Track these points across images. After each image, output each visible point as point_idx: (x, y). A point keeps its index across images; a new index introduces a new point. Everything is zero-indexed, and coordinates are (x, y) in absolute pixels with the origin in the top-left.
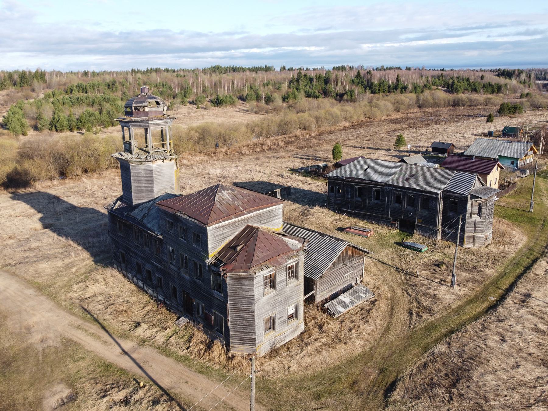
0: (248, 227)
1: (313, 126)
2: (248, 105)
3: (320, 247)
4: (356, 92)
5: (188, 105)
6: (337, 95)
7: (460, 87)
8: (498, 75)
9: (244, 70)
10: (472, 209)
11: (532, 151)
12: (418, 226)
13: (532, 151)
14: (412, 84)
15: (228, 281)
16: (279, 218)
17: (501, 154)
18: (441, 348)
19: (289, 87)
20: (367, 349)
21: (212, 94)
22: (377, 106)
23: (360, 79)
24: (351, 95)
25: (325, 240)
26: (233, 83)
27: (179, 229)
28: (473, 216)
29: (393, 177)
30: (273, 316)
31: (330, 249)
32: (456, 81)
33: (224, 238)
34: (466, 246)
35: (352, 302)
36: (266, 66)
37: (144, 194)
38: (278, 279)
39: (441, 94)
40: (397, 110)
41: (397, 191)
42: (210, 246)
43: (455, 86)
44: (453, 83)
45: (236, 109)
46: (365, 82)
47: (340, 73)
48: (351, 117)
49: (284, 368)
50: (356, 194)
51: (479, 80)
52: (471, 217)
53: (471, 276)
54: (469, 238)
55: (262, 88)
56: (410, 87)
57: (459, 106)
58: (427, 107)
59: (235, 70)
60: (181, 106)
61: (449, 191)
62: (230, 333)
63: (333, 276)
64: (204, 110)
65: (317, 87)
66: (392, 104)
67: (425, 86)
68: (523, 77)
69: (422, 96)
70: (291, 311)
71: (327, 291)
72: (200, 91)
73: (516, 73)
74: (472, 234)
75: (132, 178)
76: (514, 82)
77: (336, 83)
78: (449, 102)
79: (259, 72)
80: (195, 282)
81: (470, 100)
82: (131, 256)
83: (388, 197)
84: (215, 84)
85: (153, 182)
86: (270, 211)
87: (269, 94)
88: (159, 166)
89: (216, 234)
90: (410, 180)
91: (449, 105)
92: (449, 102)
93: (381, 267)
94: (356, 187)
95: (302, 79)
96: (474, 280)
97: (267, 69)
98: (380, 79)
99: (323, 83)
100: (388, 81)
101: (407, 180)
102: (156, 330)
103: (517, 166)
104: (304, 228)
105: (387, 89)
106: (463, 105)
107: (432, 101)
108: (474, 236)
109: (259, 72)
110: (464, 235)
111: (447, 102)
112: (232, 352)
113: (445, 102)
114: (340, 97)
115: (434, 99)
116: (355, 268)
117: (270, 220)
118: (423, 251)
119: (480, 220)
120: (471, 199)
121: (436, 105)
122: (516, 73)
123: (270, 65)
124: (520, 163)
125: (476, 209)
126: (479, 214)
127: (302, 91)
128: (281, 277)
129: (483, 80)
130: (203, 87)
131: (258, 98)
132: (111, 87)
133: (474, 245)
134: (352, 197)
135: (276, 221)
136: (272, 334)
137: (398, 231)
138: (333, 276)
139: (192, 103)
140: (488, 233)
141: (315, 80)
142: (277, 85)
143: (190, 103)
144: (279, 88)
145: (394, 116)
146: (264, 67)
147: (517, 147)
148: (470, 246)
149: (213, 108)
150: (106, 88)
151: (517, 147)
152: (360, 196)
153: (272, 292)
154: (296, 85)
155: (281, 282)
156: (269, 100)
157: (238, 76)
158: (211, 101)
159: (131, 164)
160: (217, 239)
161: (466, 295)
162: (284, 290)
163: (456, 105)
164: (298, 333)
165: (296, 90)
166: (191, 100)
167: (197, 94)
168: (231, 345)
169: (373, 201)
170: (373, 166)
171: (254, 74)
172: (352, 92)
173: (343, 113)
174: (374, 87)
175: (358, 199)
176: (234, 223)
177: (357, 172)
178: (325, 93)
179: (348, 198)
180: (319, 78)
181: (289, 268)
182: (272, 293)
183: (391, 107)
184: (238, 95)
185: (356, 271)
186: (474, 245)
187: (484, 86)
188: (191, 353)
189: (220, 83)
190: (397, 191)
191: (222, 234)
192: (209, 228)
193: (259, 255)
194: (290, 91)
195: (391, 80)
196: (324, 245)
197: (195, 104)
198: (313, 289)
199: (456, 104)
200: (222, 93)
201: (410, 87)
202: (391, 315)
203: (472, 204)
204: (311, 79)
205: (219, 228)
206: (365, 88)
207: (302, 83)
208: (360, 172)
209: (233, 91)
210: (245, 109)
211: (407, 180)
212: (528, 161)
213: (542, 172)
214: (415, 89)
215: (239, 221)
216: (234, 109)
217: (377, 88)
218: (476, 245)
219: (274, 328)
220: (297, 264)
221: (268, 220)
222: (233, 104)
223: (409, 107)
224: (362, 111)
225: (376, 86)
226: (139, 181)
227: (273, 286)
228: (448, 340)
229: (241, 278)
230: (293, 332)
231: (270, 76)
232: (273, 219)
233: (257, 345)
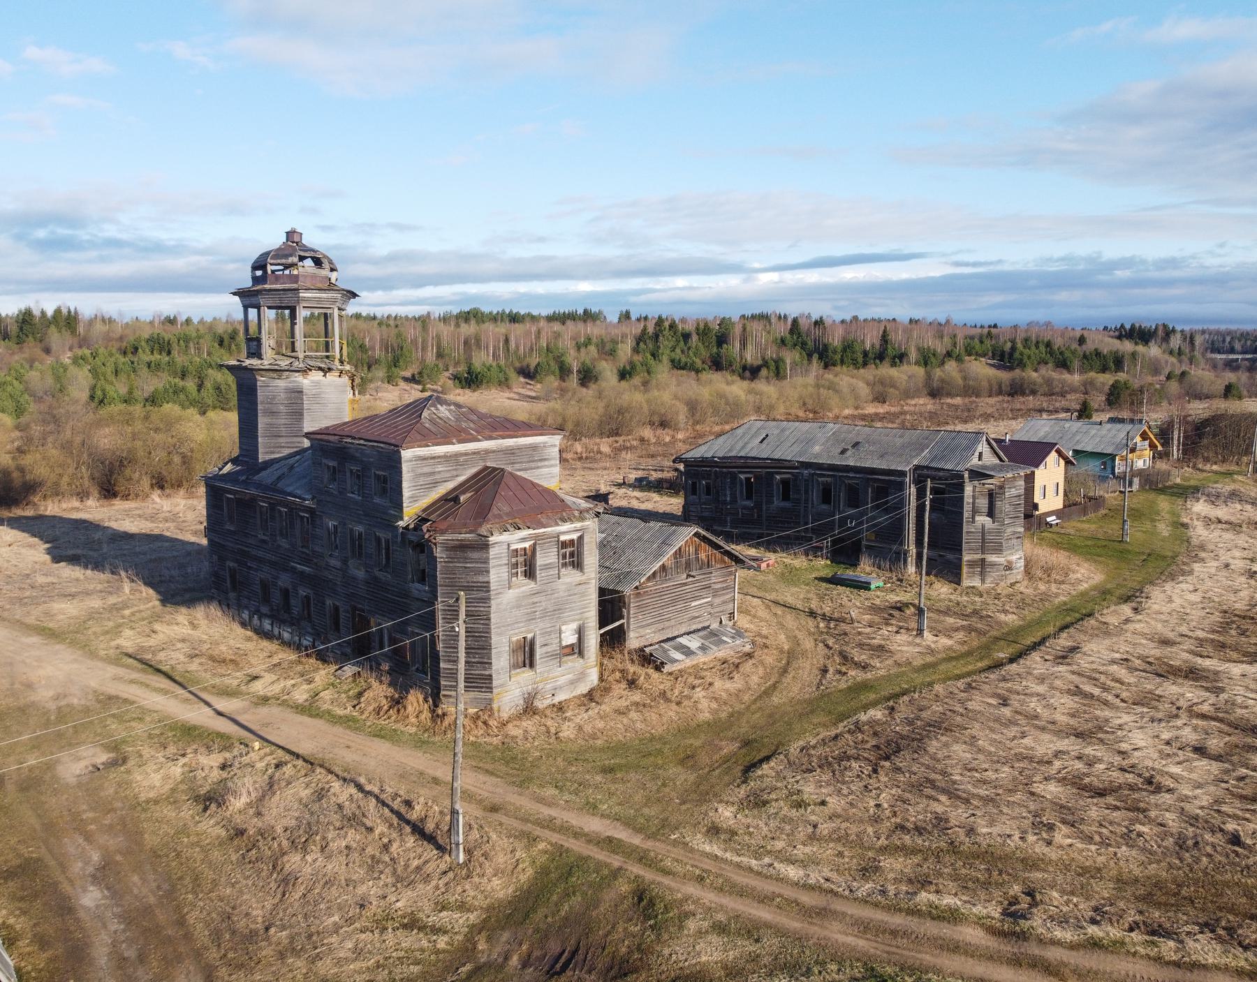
0: (486, 468)
1: (682, 418)
2: (539, 386)
3: (639, 539)
4: (788, 361)
5: (402, 384)
6: (744, 368)
7: (1029, 357)
8: (1119, 337)
9: (534, 319)
10: (974, 503)
11: (1147, 443)
12: (868, 547)
13: (1147, 443)
14: (918, 349)
15: (439, 553)
16: (552, 466)
17: (1079, 448)
18: (877, 714)
19: (636, 350)
20: (724, 715)
21: (457, 364)
22: (832, 387)
23: (799, 335)
24: (777, 368)
25: (651, 529)
26: (507, 341)
27: (348, 474)
28: (977, 518)
29: (817, 449)
30: (530, 636)
31: (660, 541)
32: (1019, 345)
33: (436, 484)
34: (966, 582)
35: (703, 648)
36: (585, 311)
37: (281, 440)
38: (540, 561)
39: (982, 369)
40: (880, 399)
41: (824, 476)
42: (406, 493)
43: (1017, 355)
44: (1013, 348)
45: (512, 395)
46: (810, 344)
47: (756, 327)
48: (771, 407)
49: (548, 732)
50: (741, 492)
51: (1075, 346)
52: (973, 518)
53: (965, 623)
54: (972, 564)
55: (573, 352)
56: (913, 355)
57: (1023, 394)
58: (949, 395)
59: (514, 318)
60: (386, 385)
61: (927, 467)
62: (442, 665)
63: (667, 598)
65: (700, 351)
66: (868, 384)
67: (949, 354)
68: (1176, 342)
69: (938, 373)
70: (570, 638)
71: (653, 628)
72: (431, 357)
73: (1160, 332)
74: (979, 556)
75: (260, 407)
76: (1154, 350)
77: (744, 344)
78: (1000, 387)
79: (569, 323)
80: (376, 578)
81: (1049, 382)
82: (250, 568)
83: (806, 492)
84: (466, 343)
85: (301, 414)
86: (534, 448)
87: (588, 362)
88: (317, 384)
89: (420, 471)
90: (849, 453)
91: (1000, 393)
92: (1000, 387)
93: (779, 611)
94: (742, 476)
95: (666, 332)
96: (970, 629)
97: (588, 316)
98: (844, 339)
99: (714, 343)
100: (863, 342)
101: (843, 452)
102: (293, 682)
103: (1113, 473)
104: (648, 625)
105: (860, 360)
106: (1034, 392)
107: (960, 382)
108: (983, 560)
109: (569, 323)
110: (960, 559)
111: (995, 387)
112: (446, 706)
113: (991, 385)
114: (751, 372)
115: (965, 378)
117: (533, 465)
118: (873, 587)
119: (993, 526)
120: (971, 478)
121: (970, 390)
122: (1160, 332)
123: (595, 309)
124: (1119, 467)
125: (983, 503)
126: (991, 514)
127: (665, 359)
128: (547, 557)
129: (1084, 347)
130: (439, 347)
131: (564, 371)
132: (226, 343)
133: (983, 581)
134: (734, 500)
136: (526, 675)
137: (829, 562)
138: (667, 598)
140: (1014, 558)
141: (695, 338)
142: (608, 347)
143: (406, 379)
144: (612, 353)
145: (871, 409)
146: (580, 311)
147: (1114, 432)
148: (976, 582)
149: (459, 391)
150: (216, 345)
151: (1114, 432)
152: (749, 497)
153: (527, 586)
154: (651, 346)
155: (547, 567)
156: (587, 376)
157: (518, 329)
158: (456, 377)
159: (258, 377)
160: (422, 481)
161: (950, 648)
163: (1016, 393)
164: (583, 689)
165: (649, 357)
166: (408, 374)
167: (423, 361)
168: (443, 693)
169: (777, 503)
170: (776, 432)
171: (557, 327)
172: (778, 363)
173: (751, 398)
174: (830, 354)
175: (748, 503)
176: (457, 455)
177: (743, 448)
178: (717, 364)
179: (725, 503)
180: (704, 331)
181: (564, 545)
182: (524, 586)
183: (864, 390)
184: (517, 365)
185: (718, 601)
186: (983, 581)
187: (1085, 356)
188: (362, 713)
189: (478, 341)
190: (824, 476)
191: (433, 473)
192: (406, 454)
193: (501, 506)
194: (637, 358)
195: (871, 340)
196: (647, 536)
197: (418, 382)
198: (622, 617)
199: (1016, 390)
200: (481, 359)
201: (913, 355)
202: (784, 671)
203: (974, 491)
204: (686, 336)
205: (425, 459)
206: (810, 356)
207: (666, 343)
208: (750, 446)
209: (507, 358)
210: (533, 394)
211: (843, 452)
212: (1140, 464)
213: (1171, 487)
214: (926, 359)
215: (466, 454)
216: (507, 395)
217: (838, 357)
218: (988, 580)
219: (532, 665)
220: (581, 538)
221: (527, 465)
222: (504, 383)
223: (907, 394)
224: (796, 396)
225: (835, 352)
226: (272, 413)
227: (530, 573)
228: (891, 703)
229: (463, 547)
230: (573, 683)
231: (593, 330)
232: (540, 464)
233: (495, 690)
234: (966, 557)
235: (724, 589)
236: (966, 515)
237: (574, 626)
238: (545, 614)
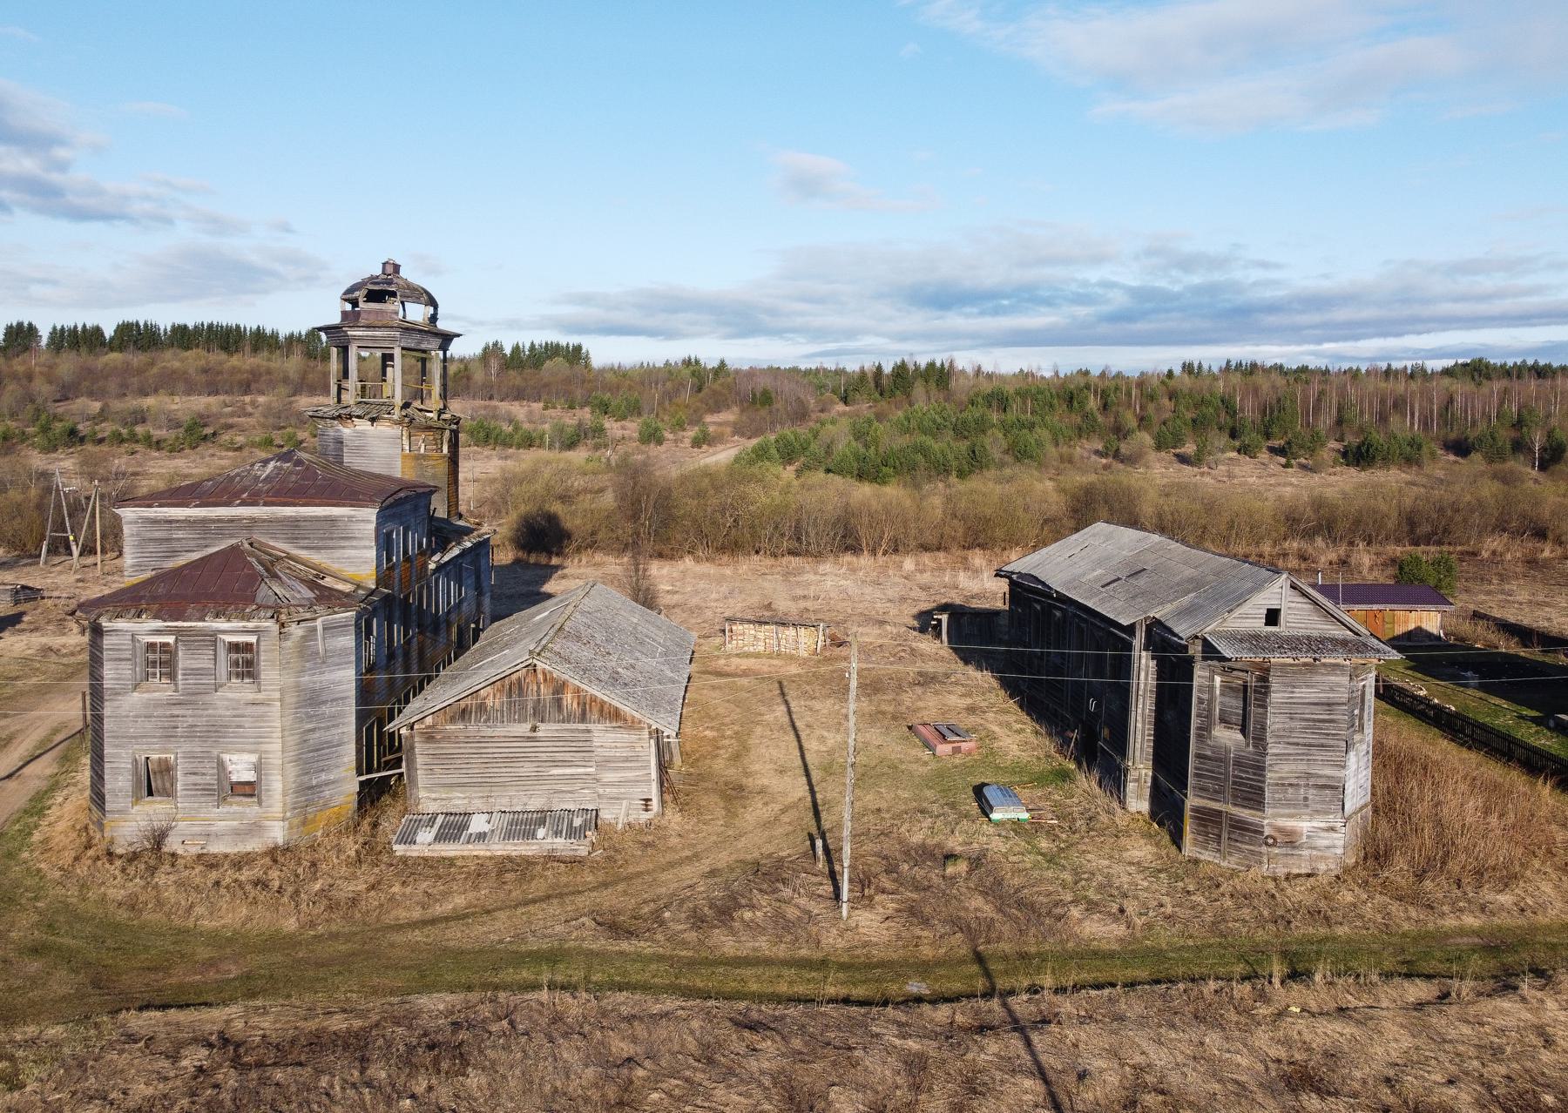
5: (1264, 456)
34: (1189, 849)
38: (184, 661)
64: (1301, 473)
72: (1326, 421)
117: (331, 543)
135: (352, 553)
139: (1280, 451)
143: (1272, 450)
162: (207, 698)
166: (1277, 443)
176: (204, 521)
230: (236, 833)
232: (343, 543)
234: (1192, 801)
235: (627, 760)
236: (1195, 722)
237: (254, 758)
238: (191, 734)
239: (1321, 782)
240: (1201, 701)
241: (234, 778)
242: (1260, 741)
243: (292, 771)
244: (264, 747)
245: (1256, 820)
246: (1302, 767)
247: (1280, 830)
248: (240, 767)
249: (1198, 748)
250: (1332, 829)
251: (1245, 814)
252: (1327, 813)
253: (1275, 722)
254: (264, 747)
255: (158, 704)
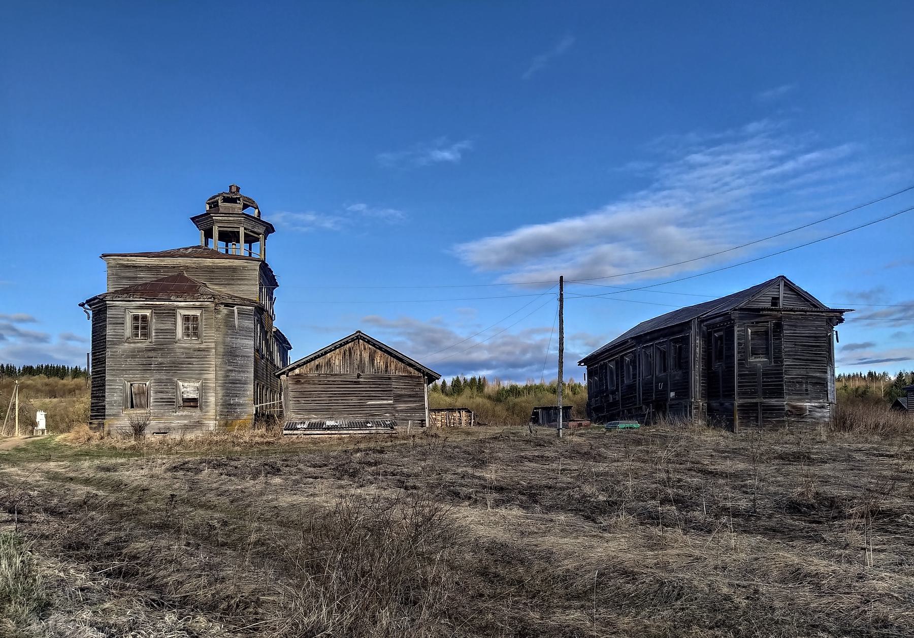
110: (733, 404)
116: (398, 398)
135: (246, 287)
230: (186, 428)
234: (738, 402)
235: (410, 396)
238: (160, 367)
239: (814, 381)
240: (739, 344)
241: (185, 396)
242: (778, 359)
243: (221, 393)
244: (206, 376)
245: (779, 403)
246: (803, 372)
247: (794, 407)
248: (188, 389)
249: (739, 371)
250: (823, 407)
251: (773, 402)
252: (820, 399)
253: (786, 346)
254: (206, 376)
255: (140, 350)
